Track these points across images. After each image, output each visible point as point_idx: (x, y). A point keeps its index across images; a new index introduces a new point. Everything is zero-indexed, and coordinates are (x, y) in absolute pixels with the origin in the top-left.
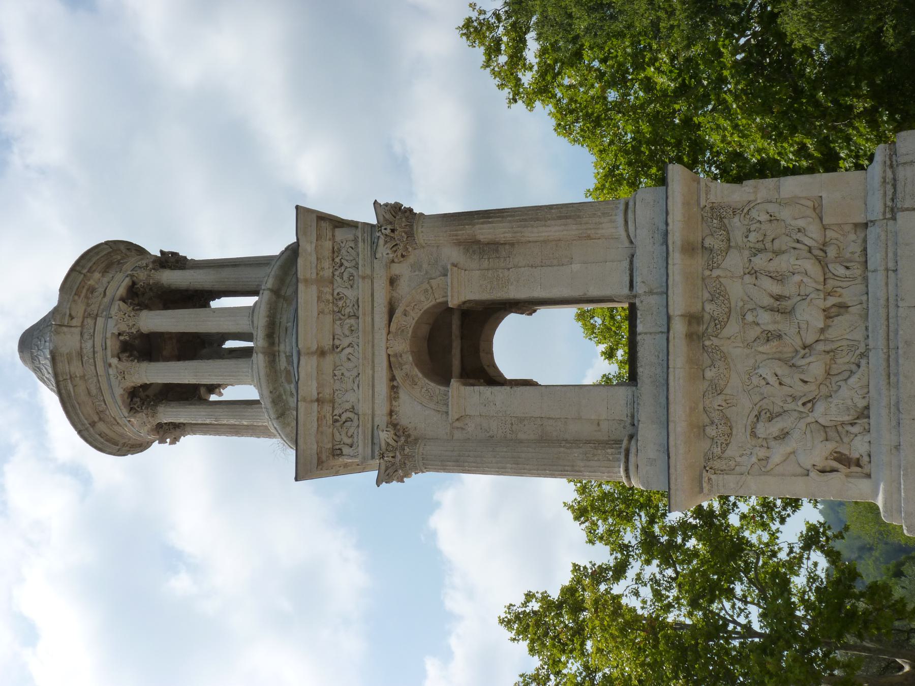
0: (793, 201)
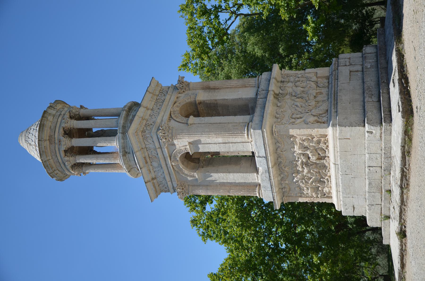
0: (310, 73)
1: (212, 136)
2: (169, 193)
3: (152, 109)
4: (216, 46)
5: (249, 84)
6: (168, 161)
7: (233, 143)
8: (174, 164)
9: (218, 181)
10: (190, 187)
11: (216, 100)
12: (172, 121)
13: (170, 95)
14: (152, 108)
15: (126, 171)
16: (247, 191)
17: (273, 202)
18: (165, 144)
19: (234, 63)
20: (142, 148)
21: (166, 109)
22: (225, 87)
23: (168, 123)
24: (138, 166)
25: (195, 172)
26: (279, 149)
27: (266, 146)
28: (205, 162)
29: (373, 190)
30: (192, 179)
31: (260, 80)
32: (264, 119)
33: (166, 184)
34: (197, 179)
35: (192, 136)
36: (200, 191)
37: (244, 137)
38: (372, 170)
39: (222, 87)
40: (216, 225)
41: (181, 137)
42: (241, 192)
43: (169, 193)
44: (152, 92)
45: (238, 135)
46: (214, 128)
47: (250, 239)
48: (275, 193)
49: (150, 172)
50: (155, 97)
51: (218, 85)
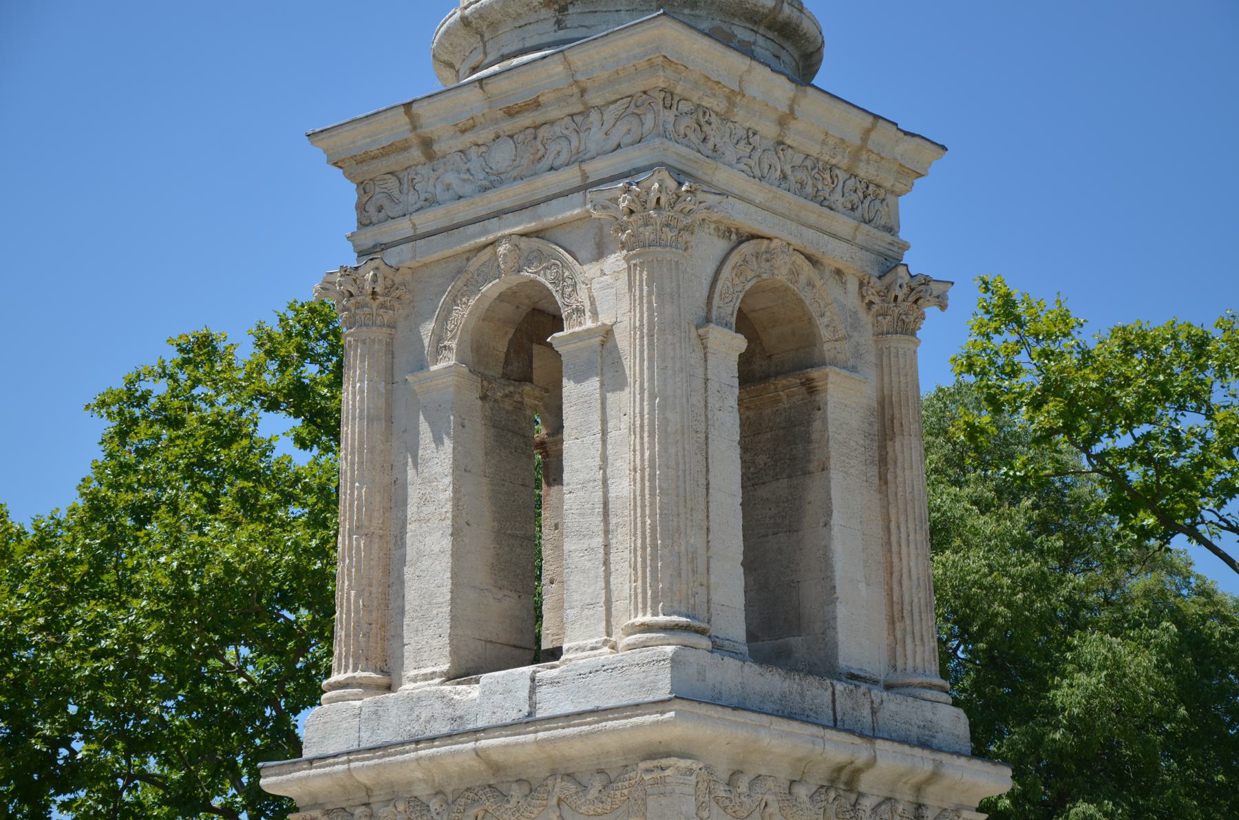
1: (642, 444)
2: (356, 224)
3: (783, 143)
4: (1106, 474)
5: (909, 640)
6: (516, 225)
7: (607, 553)
8: (501, 250)
9: (411, 472)
10: (381, 334)
11: (824, 468)
12: (722, 245)
13: (854, 237)
14: (789, 142)
15: (466, 8)
16: (358, 624)
17: (301, 756)
18: (604, 208)
19: (1014, 565)
20: (583, 92)
21: (783, 216)
22: (893, 519)
23: (713, 226)
24: (496, 68)
25: (461, 360)
26: (573, 788)
27: (589, 724)
28: (511, 408)
30: (426, 342)
31: (929, 694)
32: (729, 710)
33: (398, 210)
34: (422, 366)
35: (642, 345)
36: (361, 381)
37: (636, 609)
39: (891, 498)
40: (186, 461)
41: (641, 290)
42: (353, 593)
43: (353, 226)
44: (870, 145)
45: (644, 577)
46: (684, 456)
47: (108, 636)
48: (346, 766)
49: (463, 131)
50: (846, 161)
51: (900, 479)
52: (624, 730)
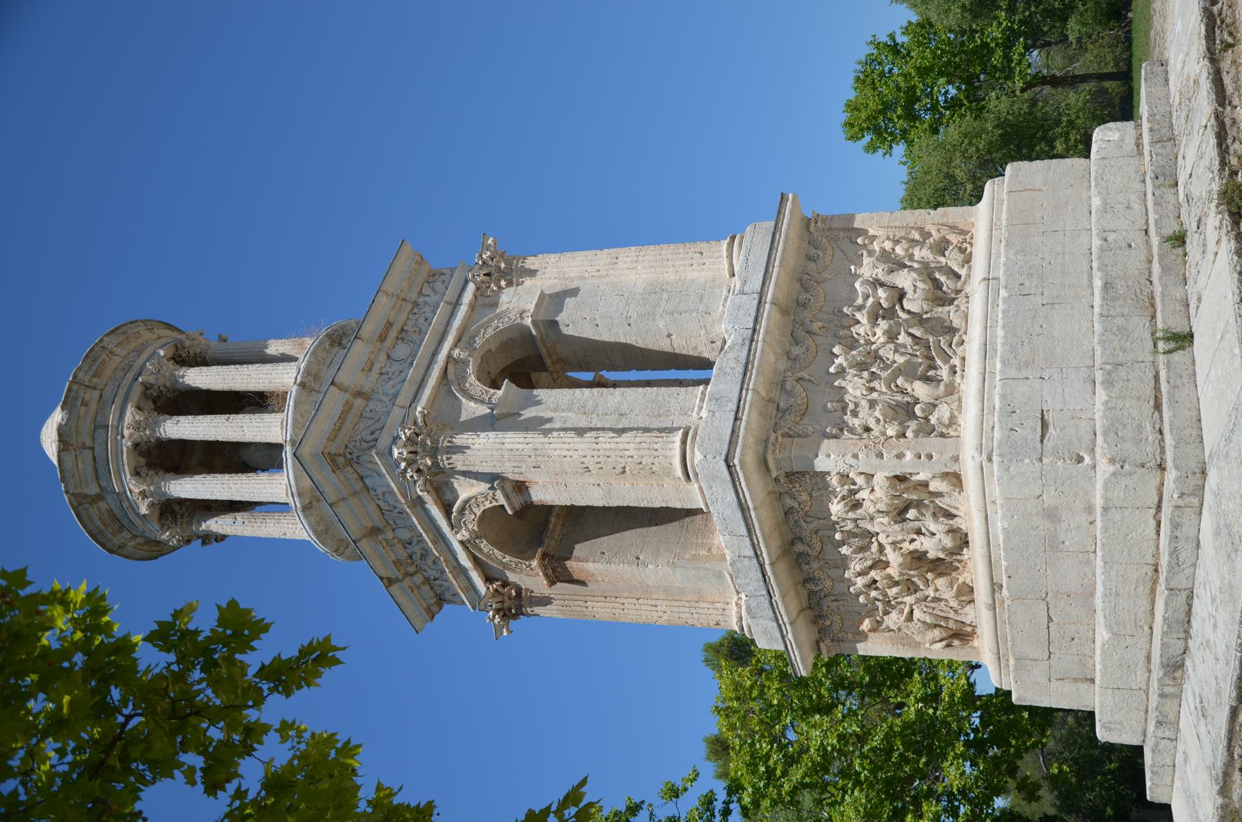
29: (1121, 306)
38: (1115, 240)
48: (750, 392)
52: (791, 219)
